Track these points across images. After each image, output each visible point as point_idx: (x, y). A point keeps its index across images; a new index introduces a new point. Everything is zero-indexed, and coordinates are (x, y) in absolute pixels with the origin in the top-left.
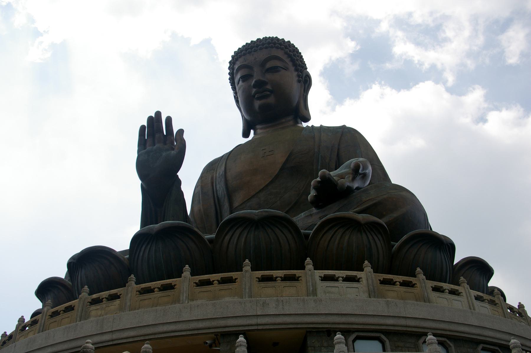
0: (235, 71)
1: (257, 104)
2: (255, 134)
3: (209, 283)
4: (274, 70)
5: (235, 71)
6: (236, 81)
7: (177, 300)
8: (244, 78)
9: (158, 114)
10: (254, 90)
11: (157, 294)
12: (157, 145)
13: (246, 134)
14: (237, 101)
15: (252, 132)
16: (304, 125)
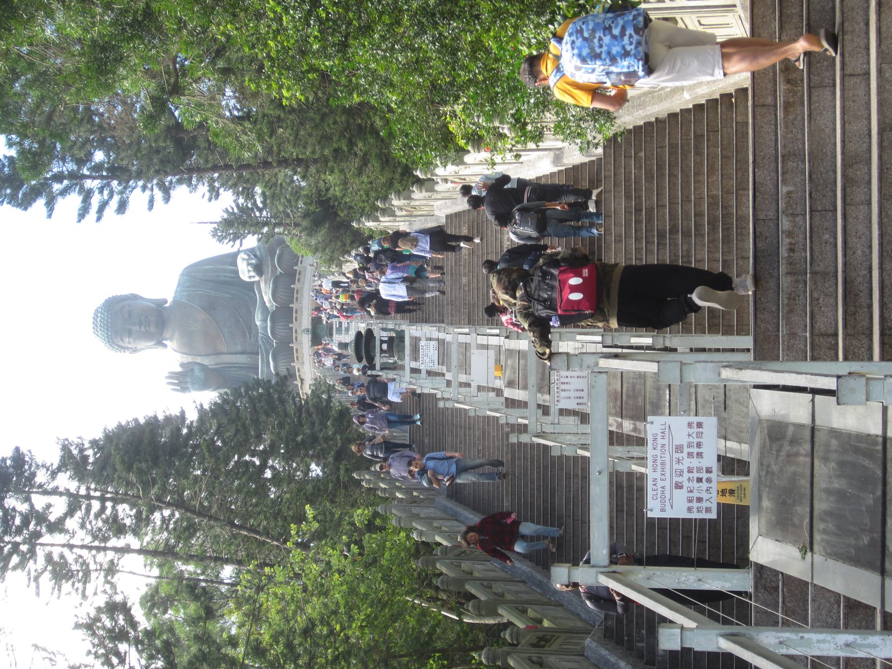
0: (121, 343)
1: (152, 329)
2: (166, 340)
3: (297, 298)
4: (130, 314)
5: (121, 343)
6: (126, 345)
7: (301, 308)
8: (130, 334)
9: (167, 377)
10: (143, 329)
11: (298, 315)
12: (188, 380)
13: (165, 346)
14: (135, 351)
15: (164, 342)
16: (167, 305)
